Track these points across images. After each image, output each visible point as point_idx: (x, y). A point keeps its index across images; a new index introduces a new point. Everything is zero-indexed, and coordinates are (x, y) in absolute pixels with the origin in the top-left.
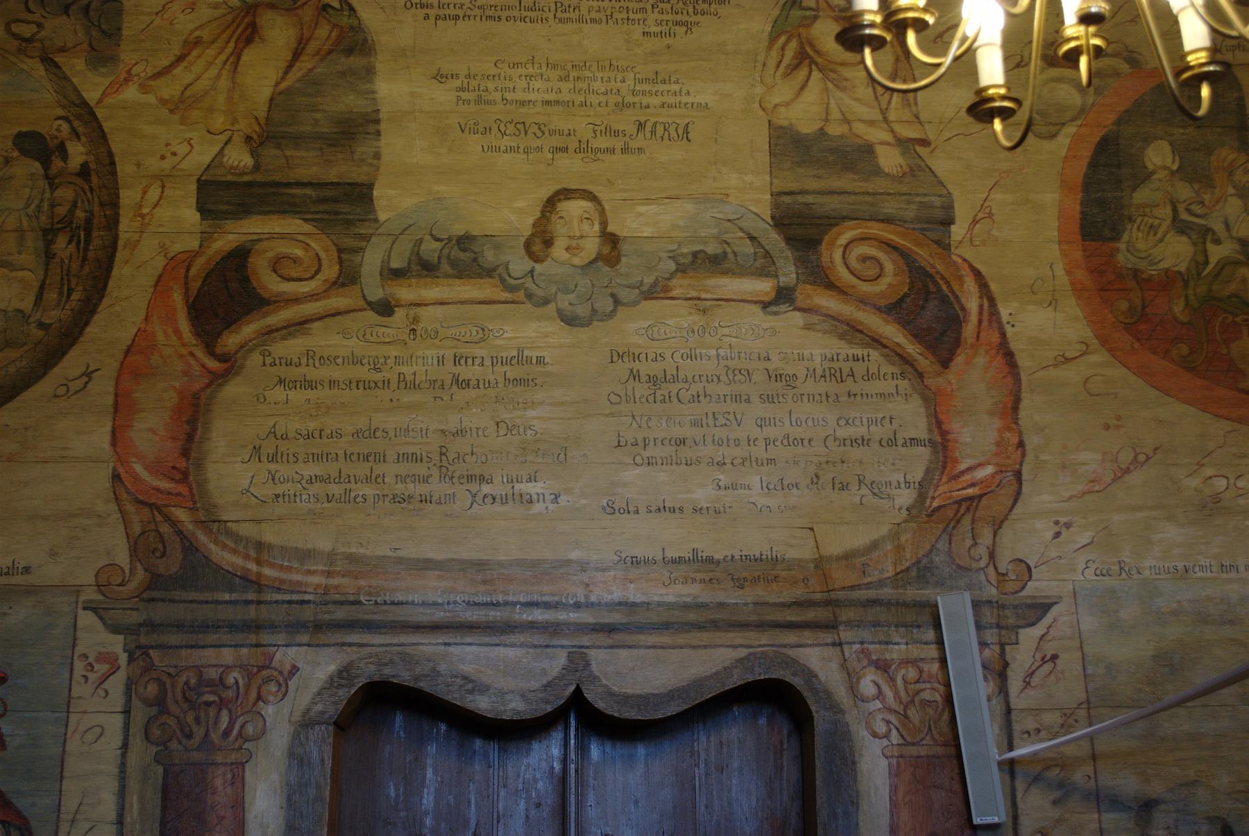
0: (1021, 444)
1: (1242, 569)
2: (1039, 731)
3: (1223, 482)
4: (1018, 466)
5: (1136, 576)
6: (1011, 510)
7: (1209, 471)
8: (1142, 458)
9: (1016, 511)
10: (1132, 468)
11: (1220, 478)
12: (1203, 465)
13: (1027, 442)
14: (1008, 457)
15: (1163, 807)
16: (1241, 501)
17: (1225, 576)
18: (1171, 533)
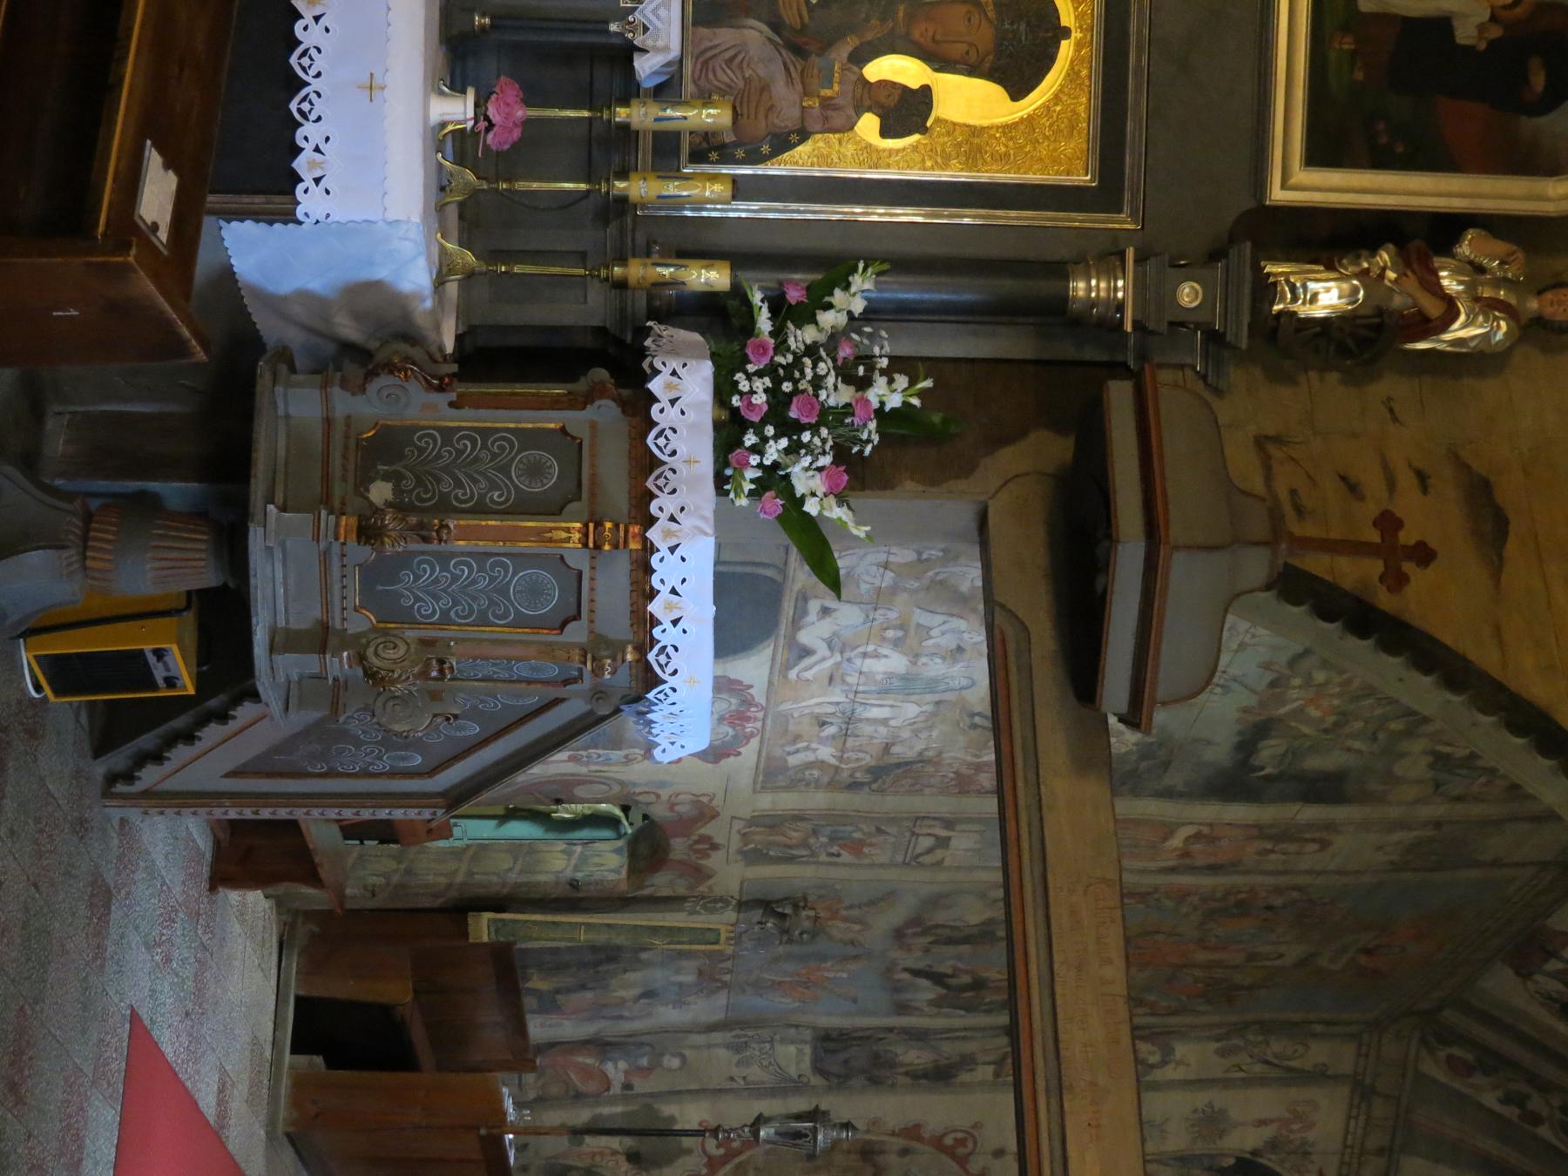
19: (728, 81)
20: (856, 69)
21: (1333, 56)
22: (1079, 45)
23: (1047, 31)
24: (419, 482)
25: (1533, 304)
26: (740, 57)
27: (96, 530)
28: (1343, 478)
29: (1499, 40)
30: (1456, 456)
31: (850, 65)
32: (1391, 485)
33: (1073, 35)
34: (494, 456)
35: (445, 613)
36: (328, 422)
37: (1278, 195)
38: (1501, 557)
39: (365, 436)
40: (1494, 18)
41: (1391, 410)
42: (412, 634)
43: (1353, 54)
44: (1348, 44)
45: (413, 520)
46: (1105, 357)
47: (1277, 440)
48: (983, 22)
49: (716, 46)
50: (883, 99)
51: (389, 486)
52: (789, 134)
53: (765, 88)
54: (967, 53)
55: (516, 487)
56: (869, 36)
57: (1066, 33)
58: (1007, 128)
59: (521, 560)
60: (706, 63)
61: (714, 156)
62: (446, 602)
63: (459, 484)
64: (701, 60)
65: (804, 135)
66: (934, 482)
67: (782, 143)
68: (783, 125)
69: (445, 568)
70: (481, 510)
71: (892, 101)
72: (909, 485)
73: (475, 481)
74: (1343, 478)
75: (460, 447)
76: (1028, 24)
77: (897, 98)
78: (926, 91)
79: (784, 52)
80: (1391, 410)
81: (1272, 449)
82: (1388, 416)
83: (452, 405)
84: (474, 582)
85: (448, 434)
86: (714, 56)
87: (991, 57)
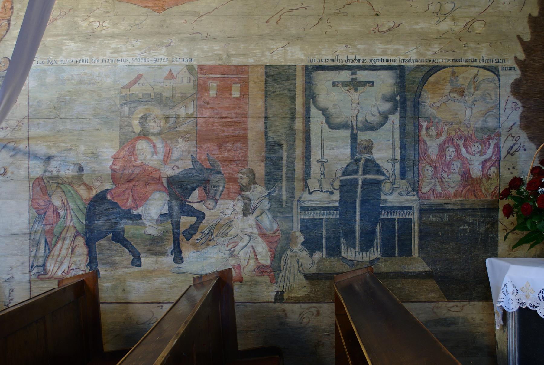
0: (12, 8)
1: (101, 61)
2: (7, 127)
3: (97, 24)
4: (9, 18)
5: (55, 64)
6: (4, 37)
7: (92, 19)
8: (63, 14)
9: (6, 37)
10: (58, 18)
11: (96, 22)
12: (90, 16)
13: (15, 7)
14: (6, 14)
15: (56, 159)
16: (104, 32)
17: (93, 64)
18: (72, 45)
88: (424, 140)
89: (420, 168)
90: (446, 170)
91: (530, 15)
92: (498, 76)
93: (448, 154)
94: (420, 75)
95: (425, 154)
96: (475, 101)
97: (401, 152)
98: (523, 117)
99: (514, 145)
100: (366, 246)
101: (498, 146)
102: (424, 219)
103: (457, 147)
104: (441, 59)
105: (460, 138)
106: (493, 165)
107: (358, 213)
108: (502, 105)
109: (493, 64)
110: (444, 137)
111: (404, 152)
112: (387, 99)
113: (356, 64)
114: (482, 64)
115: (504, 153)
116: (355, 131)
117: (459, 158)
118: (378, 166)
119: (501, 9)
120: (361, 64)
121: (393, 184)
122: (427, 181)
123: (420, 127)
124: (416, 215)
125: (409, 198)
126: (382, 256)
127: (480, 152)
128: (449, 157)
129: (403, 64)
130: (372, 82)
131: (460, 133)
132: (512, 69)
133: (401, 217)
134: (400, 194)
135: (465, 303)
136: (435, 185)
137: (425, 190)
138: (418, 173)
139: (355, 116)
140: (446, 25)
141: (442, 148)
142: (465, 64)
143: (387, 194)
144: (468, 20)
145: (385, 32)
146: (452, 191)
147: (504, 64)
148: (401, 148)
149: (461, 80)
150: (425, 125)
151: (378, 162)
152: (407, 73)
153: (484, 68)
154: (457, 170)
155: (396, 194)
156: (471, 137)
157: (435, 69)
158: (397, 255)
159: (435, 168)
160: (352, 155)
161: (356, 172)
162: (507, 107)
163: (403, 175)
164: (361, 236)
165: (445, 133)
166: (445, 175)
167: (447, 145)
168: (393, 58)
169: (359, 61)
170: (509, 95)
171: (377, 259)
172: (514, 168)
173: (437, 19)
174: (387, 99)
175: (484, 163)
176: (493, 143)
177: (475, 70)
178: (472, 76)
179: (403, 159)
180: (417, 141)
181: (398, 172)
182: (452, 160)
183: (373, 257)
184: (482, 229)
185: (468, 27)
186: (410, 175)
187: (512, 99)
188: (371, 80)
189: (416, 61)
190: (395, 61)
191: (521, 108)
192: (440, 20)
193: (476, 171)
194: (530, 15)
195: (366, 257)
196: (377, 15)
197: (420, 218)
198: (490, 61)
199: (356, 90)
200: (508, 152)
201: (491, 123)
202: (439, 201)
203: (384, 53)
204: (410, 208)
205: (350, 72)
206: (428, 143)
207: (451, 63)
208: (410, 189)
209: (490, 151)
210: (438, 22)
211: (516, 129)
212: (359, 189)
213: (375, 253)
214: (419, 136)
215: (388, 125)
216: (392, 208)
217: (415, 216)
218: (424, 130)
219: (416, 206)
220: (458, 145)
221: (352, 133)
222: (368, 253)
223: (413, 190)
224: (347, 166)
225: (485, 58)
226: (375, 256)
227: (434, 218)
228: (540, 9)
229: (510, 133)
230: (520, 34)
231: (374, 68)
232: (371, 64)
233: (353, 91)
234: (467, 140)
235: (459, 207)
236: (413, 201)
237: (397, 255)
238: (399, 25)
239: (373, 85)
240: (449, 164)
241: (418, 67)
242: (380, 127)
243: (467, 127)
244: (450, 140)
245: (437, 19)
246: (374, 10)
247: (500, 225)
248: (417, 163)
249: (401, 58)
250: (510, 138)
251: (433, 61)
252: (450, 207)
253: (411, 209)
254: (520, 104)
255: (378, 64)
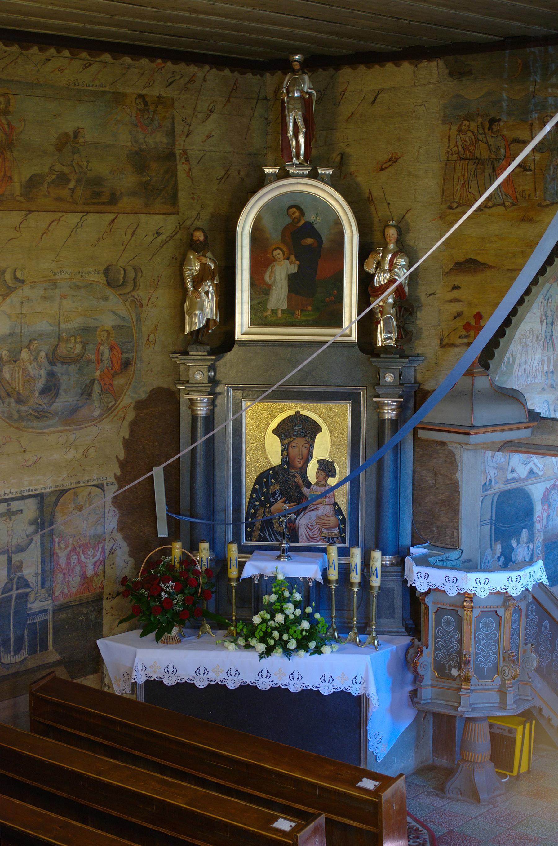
19: (317, 530)
20: (312, 486)
21: (304, 318)
22: (302, 407)
23: (297, 419)
24: (452, 660)
25: (391, 246)
26: (309, 526)
27: (468, 759)
28: (455, 318)
29: (295, 257)
30: (447, 273)
31: (311, 488)
32: (457, 300)
33: (298, 410)
34: (443, 635)
35: (494, 653)
36: (433, 686)
37: (354, 337)
38: (484, 264)
39: (437, 675)
40: (288, 259)
41: (431, 295)
42: (501, 664)
43: (302, 311)
44: (298, 312)
45: (463, 666)
46: (412, 400)
47: (442, 339)
48: (294, 442)
49: (306, 535)
50: (322, 477)
51: (453, 669)
52: (335, 509)
53: (319, 518)
54: (306, 447)
55: (453, 630)
56: (301, 482)
57: (298, 412)
58: (331, 432)
59: (477, 629)
60: (311, 538)
61: (343, 535)
62: (490, 653)
63: (452, 647)
64: (310, 540)
65: (335, 504)
66: (457, 467)
67: (339, 512)
68: (332, 511)
69: (479, 654)
70: (460, 641)
71: (323, 473)
72: (458, 475)
73: (451, 642)
74: (455, 318)
75: (440, 645)
76: (295, 426)
77: (322, 472)
78: (318, 462)
79: (306, 511)
80: (431, 295)
81: (444, 343)
82: (433, 296)
83: (427, 647)
84: (484, 644)
85: (436, 649)
86: (309, 535)
87: (307, 439)
88: (57, 553)
89: (54, 576)
90: (71, 574)
91: (124, 437)
92: (104, 491)
93: (72, 561)
94: (54, 498)
95: (58, 564)
96: (89, 514)
97: (42, 566)
98: (120, 522)
99: (114, 545)
100: (18, 651)
101: (104, 548)
102: (56, 617)
103: (78, 554)
104: (69, 483)
105: (80, 547)
106: (100, 564)
107: (12, 624)
108: (106, 515)
109: (100, 482)
110: (70, 548)
111: (43, 566)
112: (31, 523)
113: (10, 496)
114: (94, 483)
115: (107, 552)
116: (10, 556)
117: (79, 563)
118: (26, 581)
119: (105, 435)
120: (14, 496)
121: (36, 594)
122: (59, 586)
123: (53, 542)
124: (51, 615)
125: (46, 603)
126: (29, 655)
127: (93, 555)
128: (73, 564)
129: (43, 491)
130: (21, 510)
131: (80, 543)
132: (112, 484)
133: (41, 620)
134: (40, 601)
135: (83, 678)
136: (64, 588)
137: (57, 594)
138: (53, 581)
139: (10, 541)
140: (71, 454)
141: (69, 558)
142: (83, 484)
143: (31, 603)
144: (85, 447)
145: (30, 466)
146: (74, 590)
147: (108, 480)
148: (42, 562)
149: (80, 499)
150: (57, 540)
151: (26, 577)
152: (45, 498)
153: (95, 486)
154: (78, 574)
155: (38, 601)
156: (87, 545)
157: (63, 492)
158: (38, 652)
159: (64, 574)
160: (9, 575)
161: (11, 590)
162: (110, 515)
163: (43, 584)
164: (14, 643)
165: (70, 544)
166: (70, 579)
167: (72, 554)
168: (36, 487)
169: (13, 493)
170: (111, 505)
171: (25, 658)
172: (113, 564)
173: (65, 450)
174: (31, 523)
175: (95, 564)
176: (101, 546)
177: (90, 488)
178: (87, 494)
179: (43, 571)
180: (53, 554)
181: (39, 583)
182: (75, 565)
183: (23, 658)
184: (93, 617)
185: (85, 454)
186: (47, 584)
187: (113, 508)
188: (20, 508)
189: (51, 487)
190: (37, 490)
191: (118, 515)
192: (67, 450)
193: (90, 572)
194: (124, 437)
195: (18, 658)
196: (25, 451)
197: (53, 617)
198: (99, 479)
199: (11, 519)
200: (110, 552)
201: (100, 530)
202: (66, 600)
203: (30, 484)
204: (46, 611)
205: (6, 504)
206: (60, 555)
207: (74, 486)
208: (47, 595)
209: (99, 553)
210: (66, 452)
211: (115, 531)
212: (13, 603)
213: (25, 654)
214: (54, 550)
215: (33, 545)
216: (35, 614)
217: (50, 617)
218: (57, 544)
219: (50, 608)
220: (79, 552)
221: (8, 557)
222: (19, 655)
223: (49, 595)
224: (5, 585)
225: (96, 478)
226: (24, 657)
227: (63, 616)
228: (130, 432)
229: (111, 536)
230: (118, 455)
231: (23, 498)
232: (21, 495)
233: (8, 520)
234: (84, 546)
235: (78, 603)
236: (49, 604)
237: (38, 652)
238: (40, 459)
239: (22, 513)
240: (72, 570)
241: (52, 492)
242: (27, 548)
243: (85, 537)
244: (74, 550)
245: (65, 450)
246: (22, 447)
247: (104, 610)
248: (52, 573)
249: (42, 486)
250: (112, 540)
251: (63, 485)
252: (72, 604)
253: (47, 612)
254: (117, 511)
255: (26, 494)
